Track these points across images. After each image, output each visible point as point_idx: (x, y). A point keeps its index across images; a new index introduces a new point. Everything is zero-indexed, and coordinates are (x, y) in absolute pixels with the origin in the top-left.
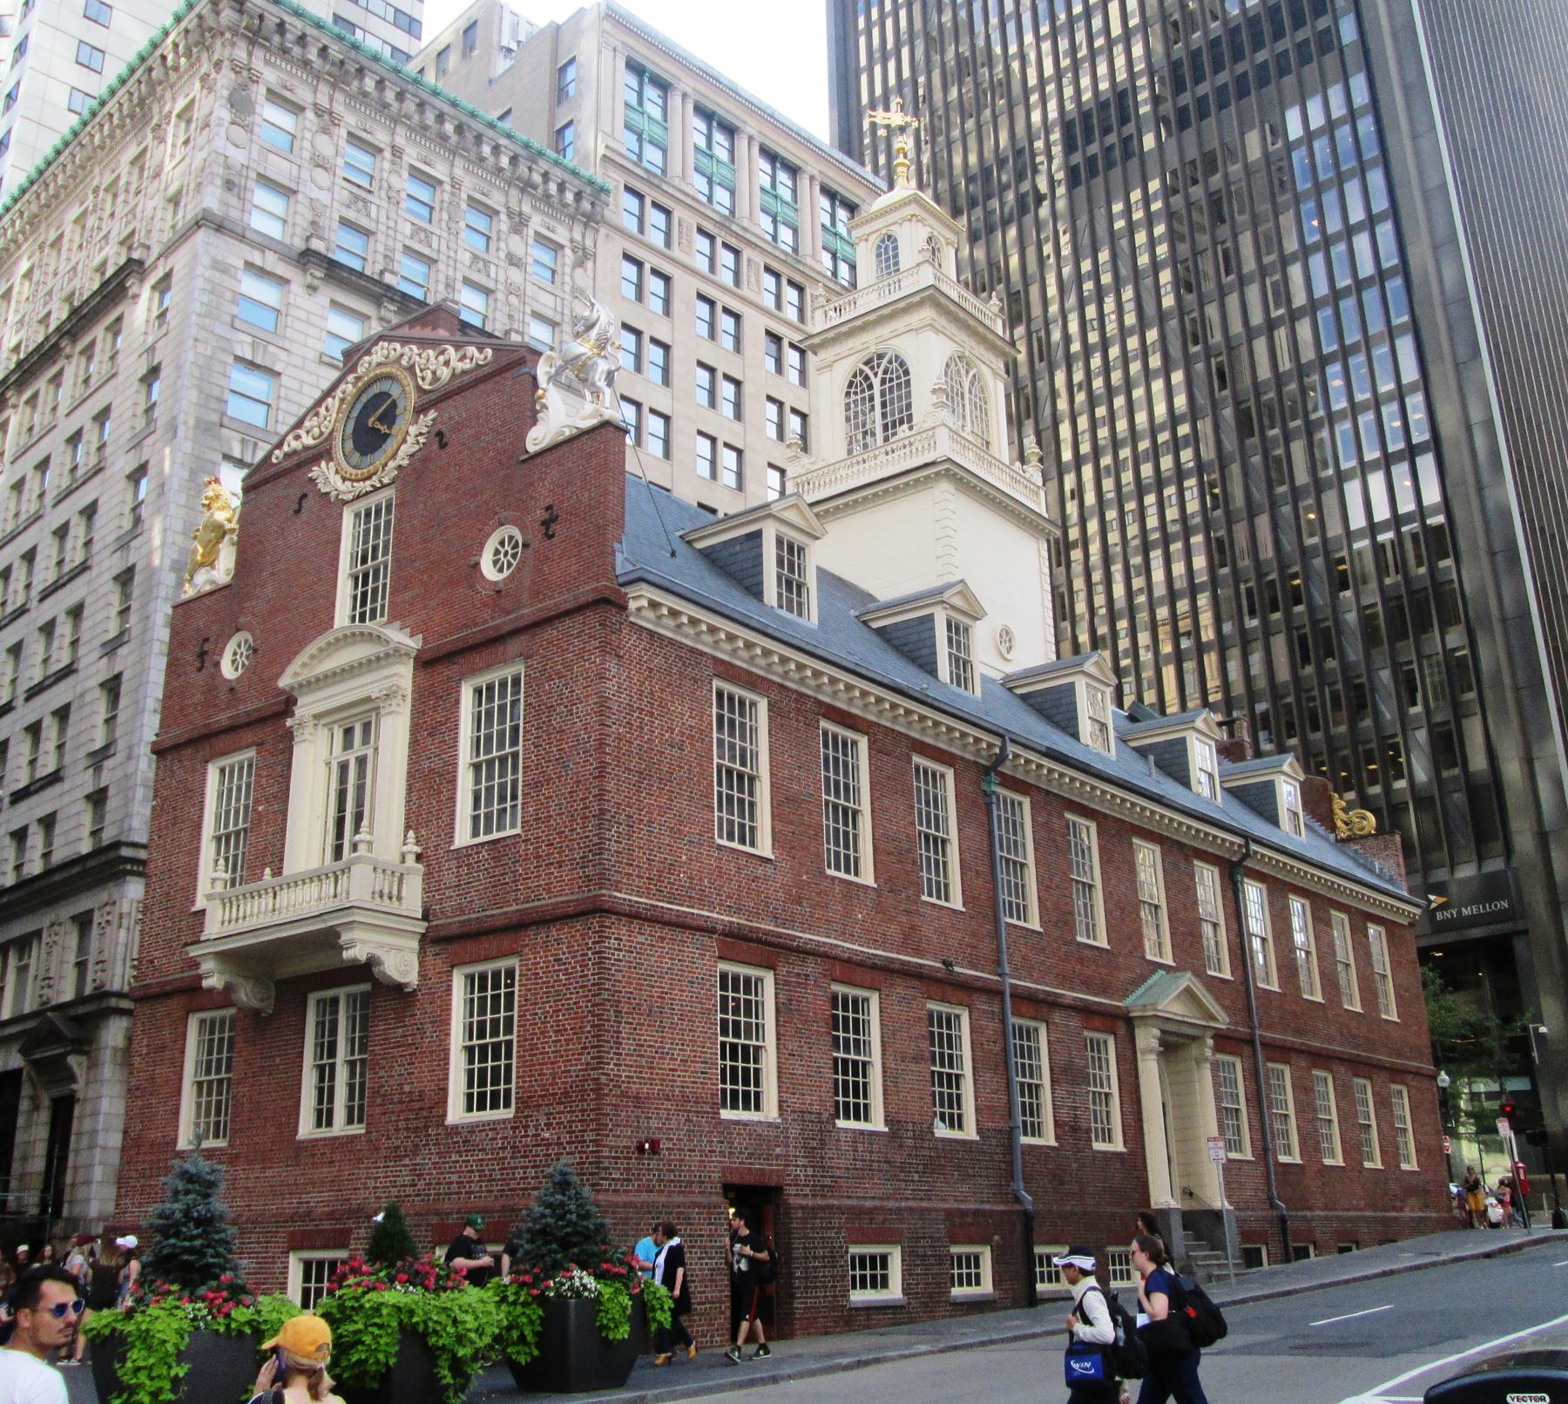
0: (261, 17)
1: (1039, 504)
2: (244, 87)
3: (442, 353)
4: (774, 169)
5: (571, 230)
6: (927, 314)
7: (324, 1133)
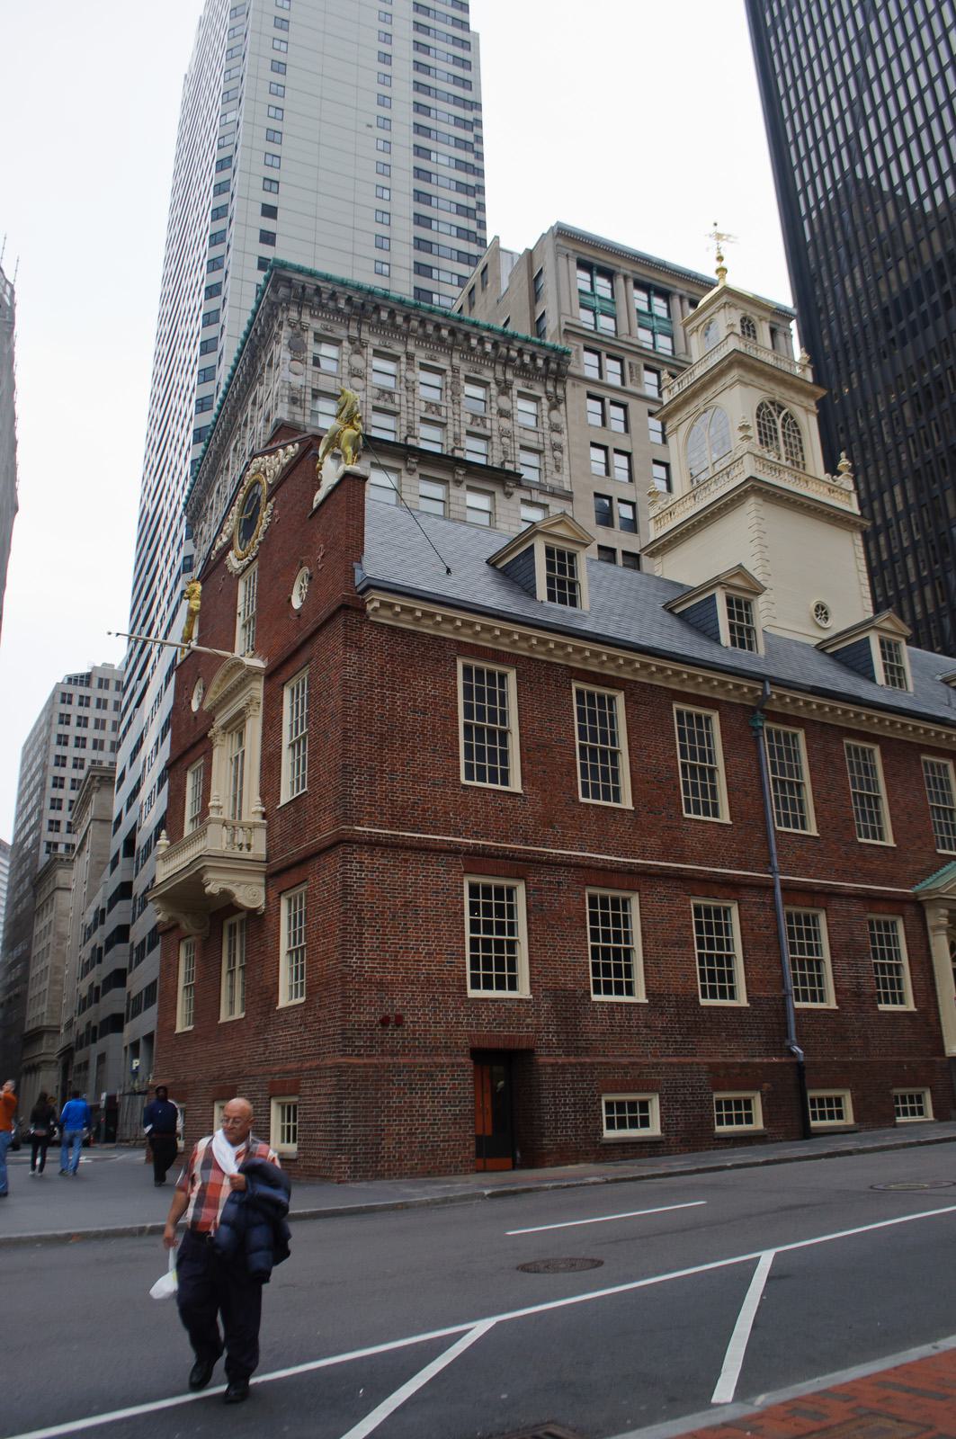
0: (304, 288)
2: (298, 335)
5: (545, 385)
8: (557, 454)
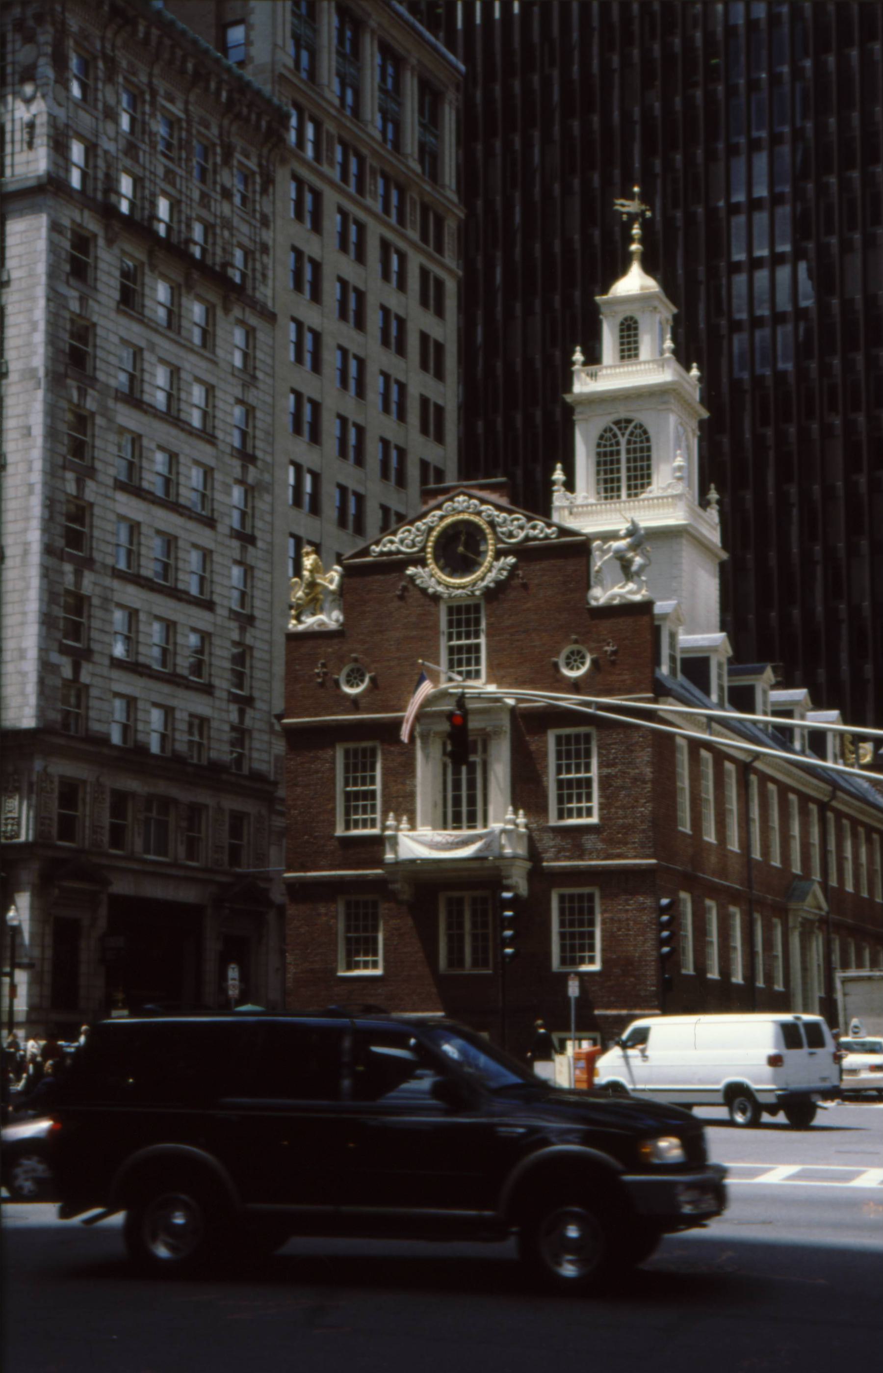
1: (714, 536)
3: (518, 519)
8: (265, 258)
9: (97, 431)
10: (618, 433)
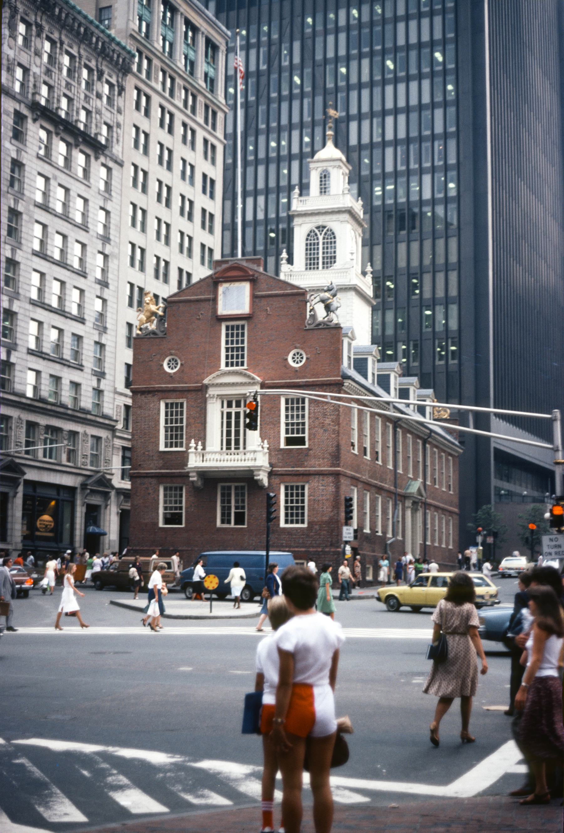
1: (370, 292)
4: (187, 28)
6: (346, 217)
7: (226, 526)
8: (119, 130)
9: (23, 223)
10: (318, 233)
